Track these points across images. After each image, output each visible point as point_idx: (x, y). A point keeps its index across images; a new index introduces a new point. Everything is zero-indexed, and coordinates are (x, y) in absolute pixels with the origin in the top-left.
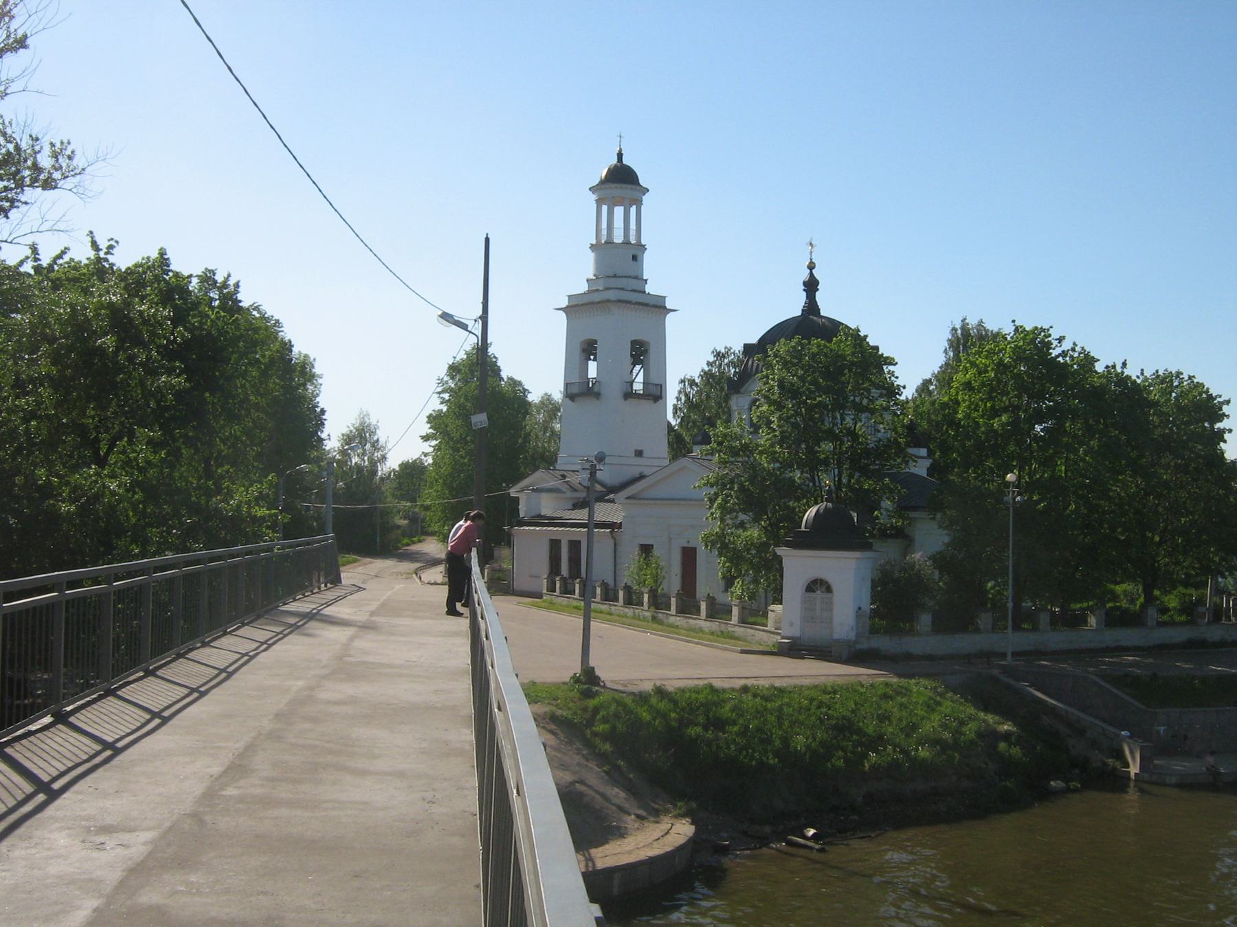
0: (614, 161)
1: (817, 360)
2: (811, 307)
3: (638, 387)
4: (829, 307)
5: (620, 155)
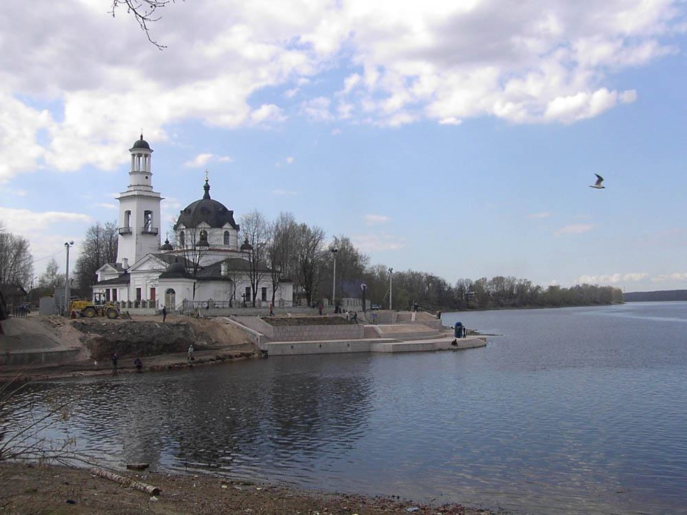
0: (139, 139)
1: (208, 214)
2: (207, 196)
4: (214, 196)
5: (142, 136)
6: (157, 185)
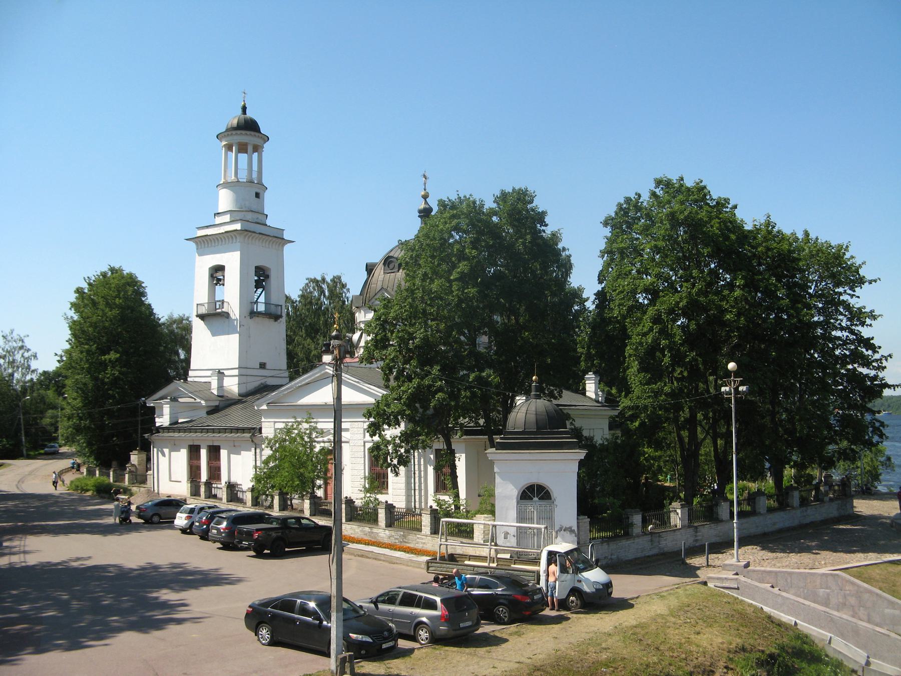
3: (261, 308)
6: (276, 215)
